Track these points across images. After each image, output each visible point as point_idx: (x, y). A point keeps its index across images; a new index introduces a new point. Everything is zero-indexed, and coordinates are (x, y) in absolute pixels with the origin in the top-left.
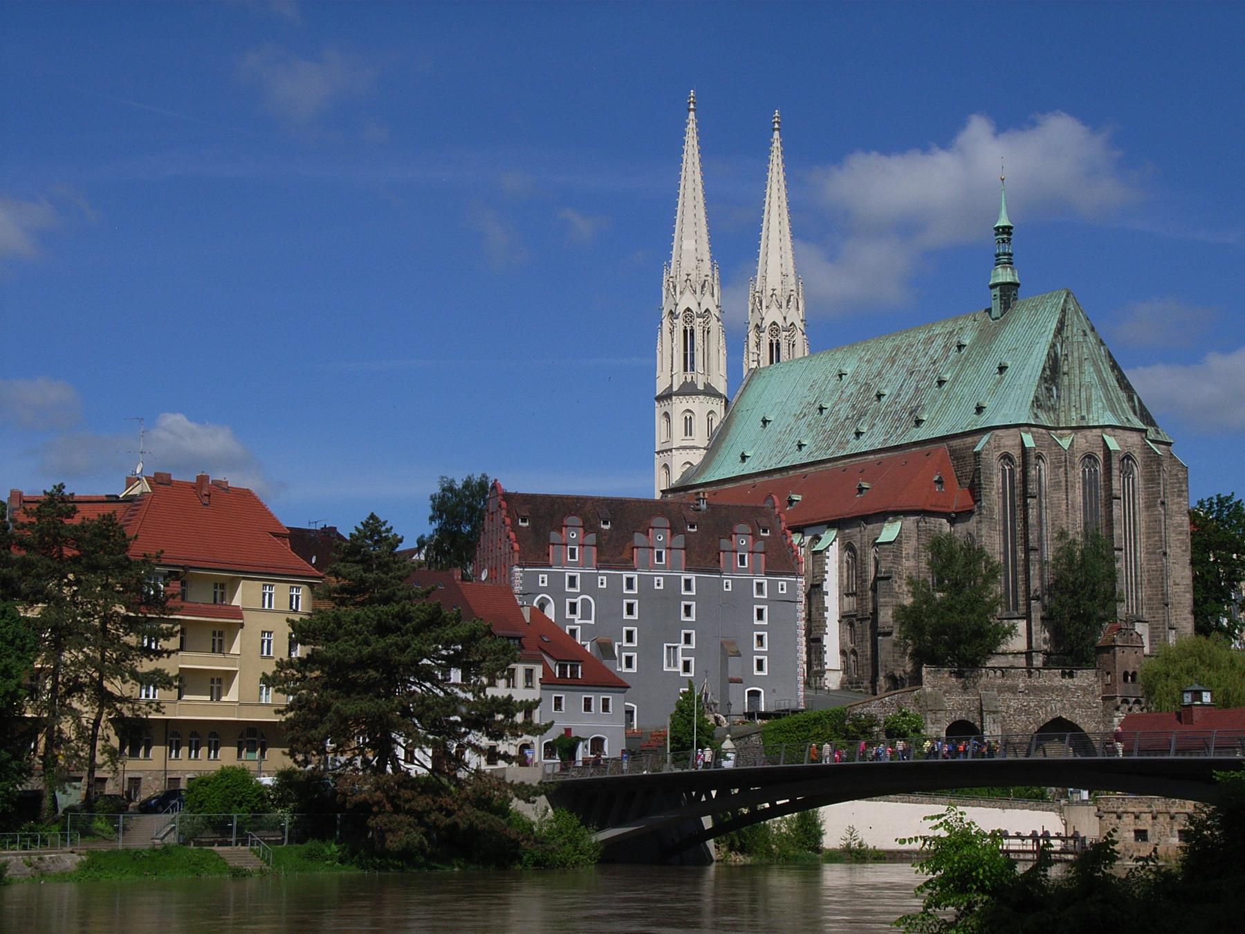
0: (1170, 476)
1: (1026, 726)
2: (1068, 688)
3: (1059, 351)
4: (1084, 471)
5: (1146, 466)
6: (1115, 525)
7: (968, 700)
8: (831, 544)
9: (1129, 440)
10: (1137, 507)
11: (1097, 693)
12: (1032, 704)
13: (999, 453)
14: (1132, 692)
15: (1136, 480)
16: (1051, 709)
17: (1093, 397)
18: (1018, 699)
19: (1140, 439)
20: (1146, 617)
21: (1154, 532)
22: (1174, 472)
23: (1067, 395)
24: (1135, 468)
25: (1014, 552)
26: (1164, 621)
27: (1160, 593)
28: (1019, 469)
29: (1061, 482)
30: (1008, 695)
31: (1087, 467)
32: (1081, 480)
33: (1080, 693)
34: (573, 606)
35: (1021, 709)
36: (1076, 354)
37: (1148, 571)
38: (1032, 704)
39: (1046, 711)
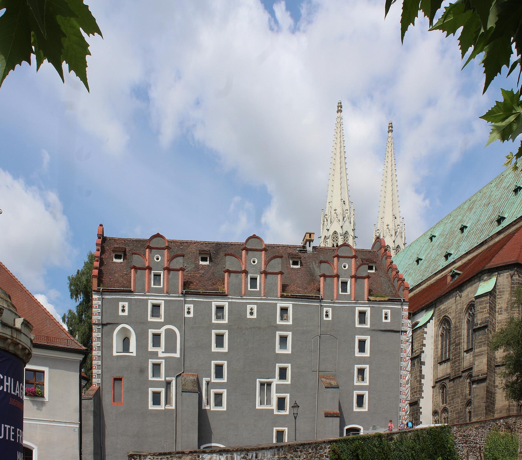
8: (429, 322)
34: (156, 337)
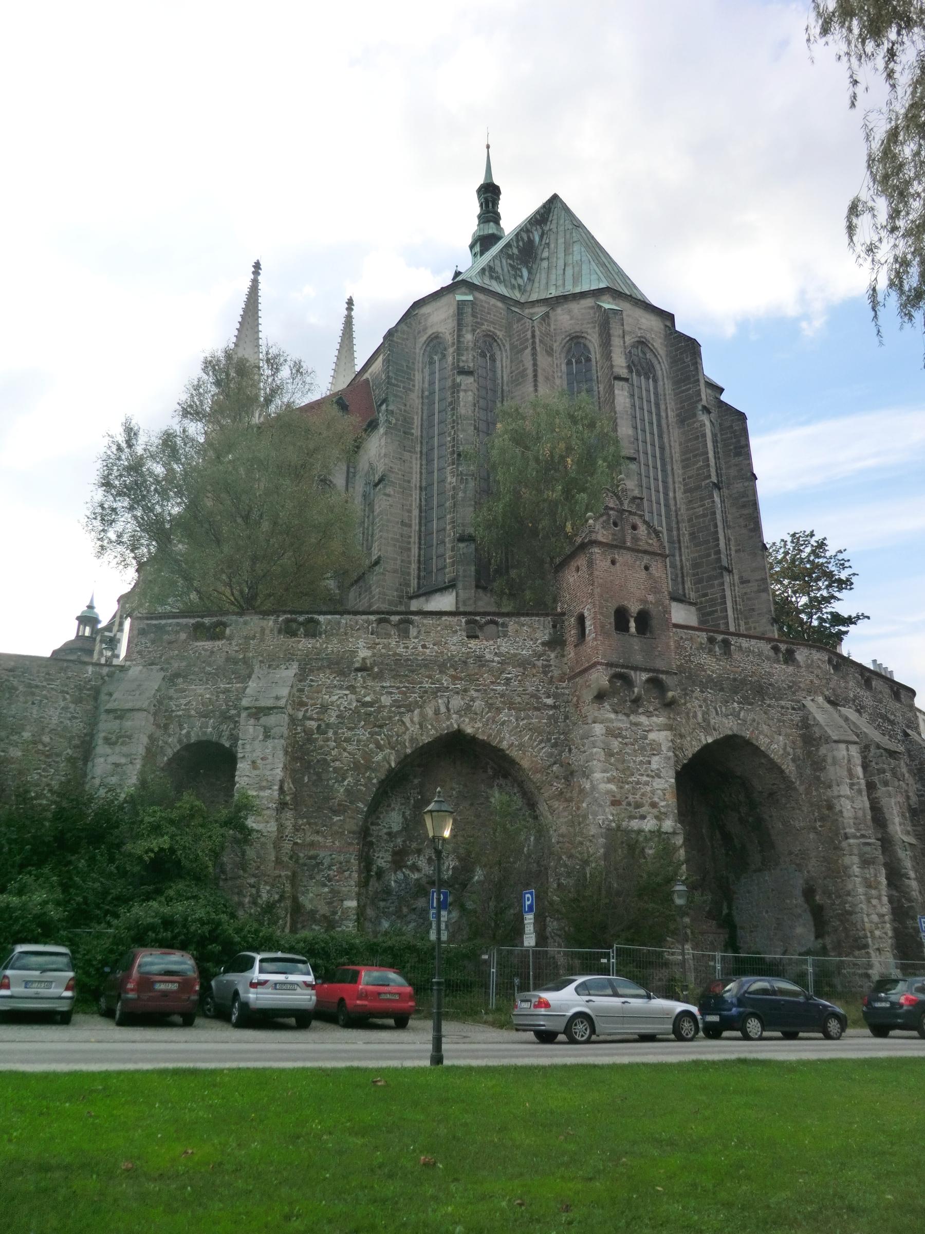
0: (721, 430)
1: (368, 756)
2: (480, 658)
3: (537, 239)
4: (569, 363)
5: (675, 361)
6: (618, 420)
7: (226, 691)
9: (643, 321)
10: (664, 422)
11: (556, 673)
12: (386, 700)
13: (425, 338)
14: (638, 658)
15: (660, 383)
16: (437, 712)
17: (584, 272)
18: (352, 689)
19: (662, 327)
20: (692, 596)
21: (695, 456)
22: (727, 424)
23: (544, 275)
24: (657, 367)
25: (442, 481)
26: (724, 597)
27: (712, 551)
28: (451, 350)
29: (525, 370)
30: (324, 678)
31: (573, 356)
32: (565, 376)
33: (512, 671)
35: (356, 711)
36: (561, 240)
37: (690, 520)
38: (386, 700)
39: (423, 716)
